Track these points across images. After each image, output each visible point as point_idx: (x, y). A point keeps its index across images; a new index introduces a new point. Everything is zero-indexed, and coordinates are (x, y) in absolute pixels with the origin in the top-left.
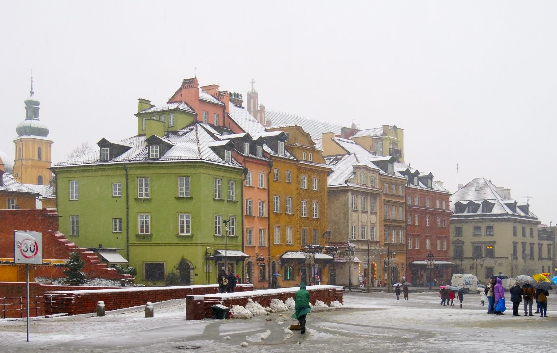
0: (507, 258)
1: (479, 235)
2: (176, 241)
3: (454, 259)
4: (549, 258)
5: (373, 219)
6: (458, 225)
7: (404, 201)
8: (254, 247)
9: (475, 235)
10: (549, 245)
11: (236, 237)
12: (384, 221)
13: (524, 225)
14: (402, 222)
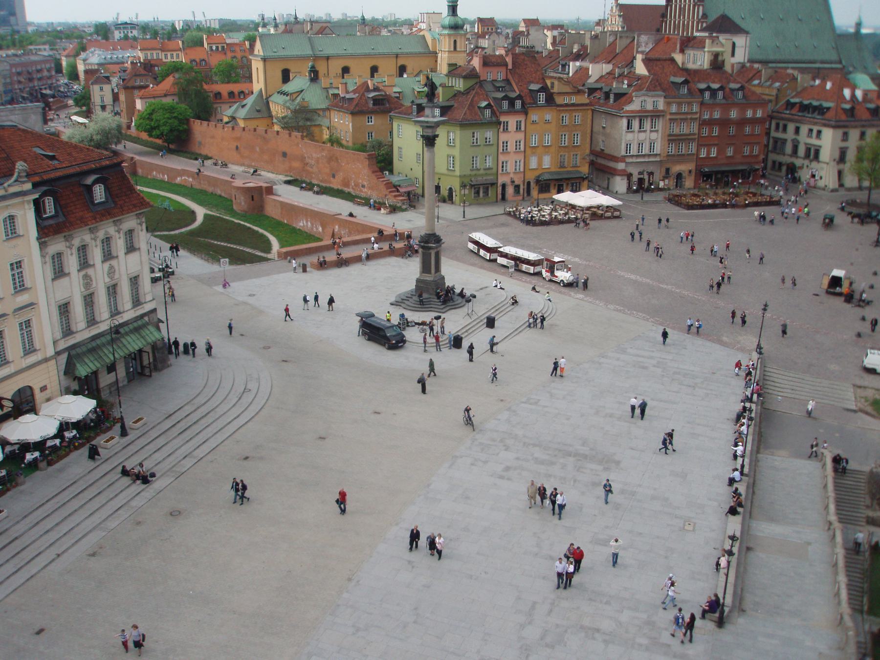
0: (828, 164)
1: (811, 137)
2: (446, 172)
3: (791, 156)
5: (654, 136)
6: (798, 125)
8: (509, 173)
12: (670, 135)
13: (863, 129)
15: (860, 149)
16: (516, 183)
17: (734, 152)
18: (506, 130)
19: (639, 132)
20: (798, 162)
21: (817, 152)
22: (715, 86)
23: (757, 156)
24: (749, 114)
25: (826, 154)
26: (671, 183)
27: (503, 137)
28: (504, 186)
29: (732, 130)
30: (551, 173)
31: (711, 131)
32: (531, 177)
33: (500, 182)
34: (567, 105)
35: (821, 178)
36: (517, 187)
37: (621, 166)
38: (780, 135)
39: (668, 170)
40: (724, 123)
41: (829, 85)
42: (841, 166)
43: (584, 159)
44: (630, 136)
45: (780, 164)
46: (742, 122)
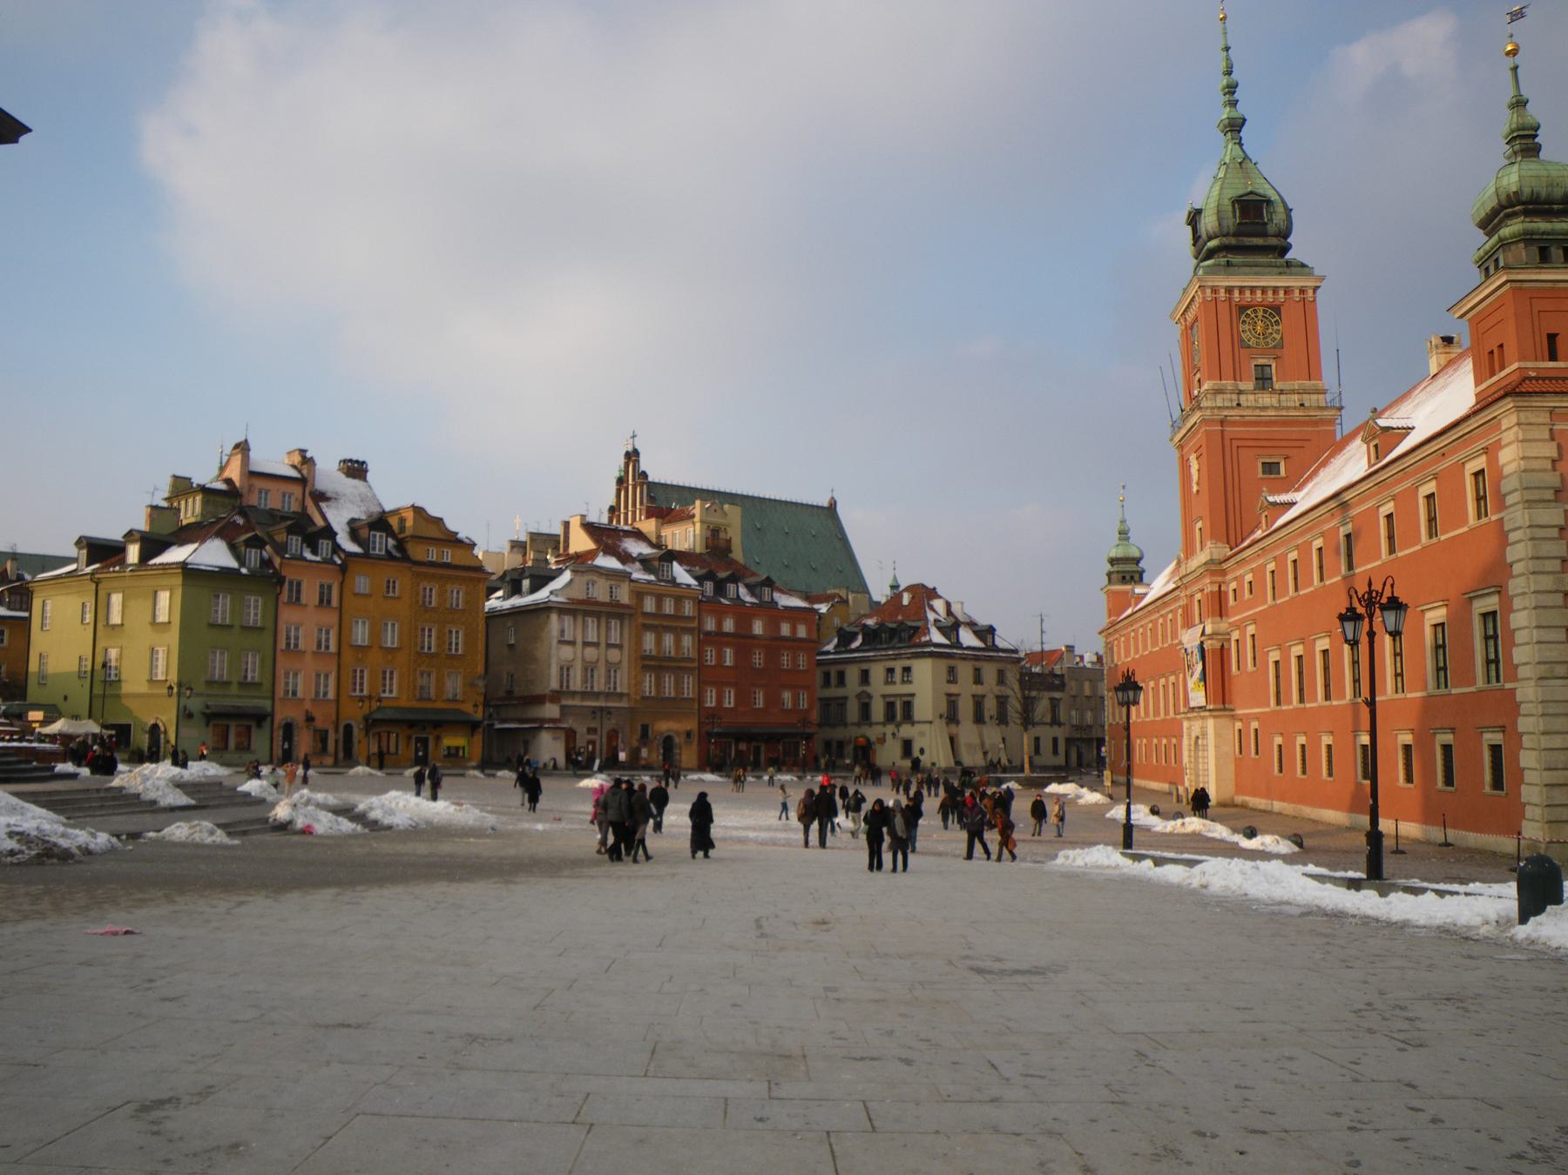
1: (893, 683)
3: (858, 724)
4: (1055, 722)
5: (614, 655)
6: (865, 666)
7: (695, 624)
9: (887, 683)
10: (1052, 699)
11: (259, 685)
12: (645, 658)
14: (692, 660)
15: (978, 702)
16: (319, 724)
17: (766, 701)
18: (296, 600)
19: (586, 644)
20: (873, 733)
21: (908, 706)
22: (722, 575)
23: (806, 711)
24: (785, 630)
25: (925, 706)
26: (654, 756)
27: (288, 615)
28: (288, 729)
29: (758, 659)
30: (397, 709)
31: (720, 656)
32: (354, 715)
33: (282, 714)
34: (433, 564)
35: (922, 751)
36: (322, 737)
37: (551, 710)
38: (834, 692)
39: (645, 728)
40: (742, 640)
41: (906, 601)
42: (953, 729)
43: (473, 685)
44: (567, 652)
45: (841, 744)
46: (774, 644)
